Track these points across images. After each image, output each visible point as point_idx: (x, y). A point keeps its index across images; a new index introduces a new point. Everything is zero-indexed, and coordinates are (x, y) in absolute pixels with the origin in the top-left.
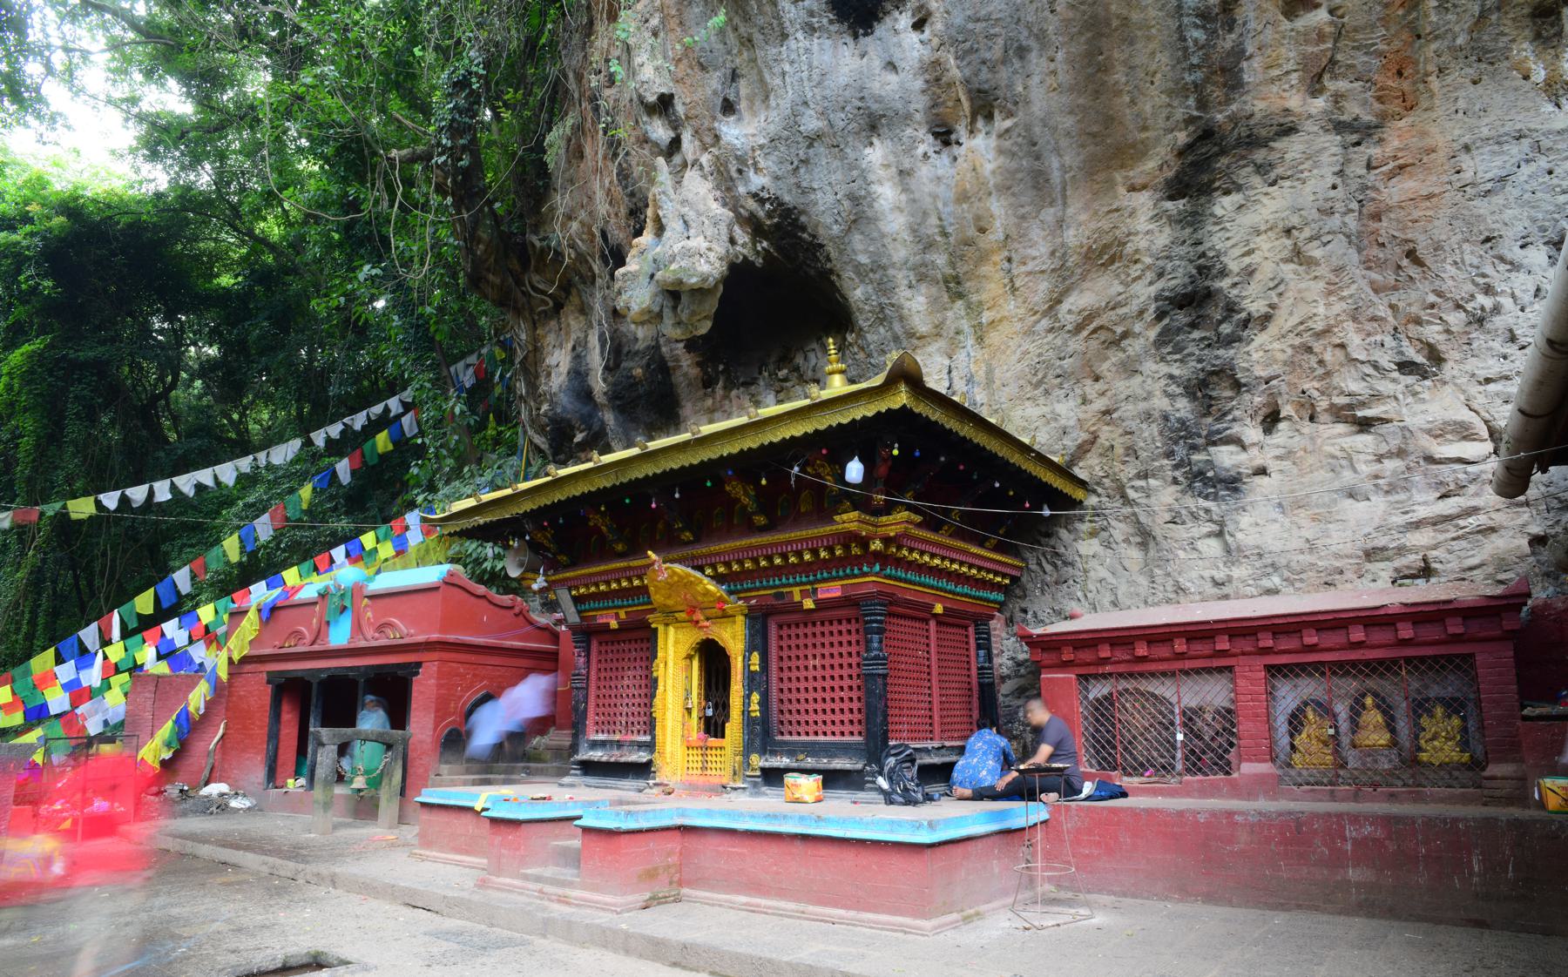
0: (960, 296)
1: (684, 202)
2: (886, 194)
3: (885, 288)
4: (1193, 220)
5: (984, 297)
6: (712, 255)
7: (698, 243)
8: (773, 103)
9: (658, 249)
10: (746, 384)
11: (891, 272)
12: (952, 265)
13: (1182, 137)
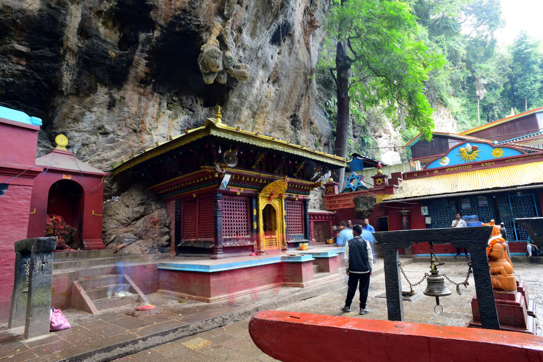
0: (254, 118)
2: (257, 84)
3: (242, 104)
4: (295, 132)
5: (258, 121)
8: (256, 38)
10: (161, 94)
11: (246, 101)
12: (257, 110)
13: (292, 113)
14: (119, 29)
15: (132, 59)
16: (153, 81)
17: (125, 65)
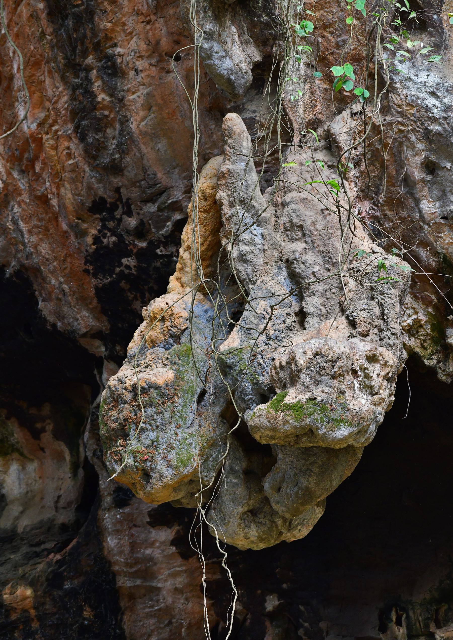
1: (295, 230)
6: (375, 370)
7: (336, 337)
9: (234, 340)
14: (57, 436)
15: (103, 565)
16: (271, 603)
17: (87, 613)
